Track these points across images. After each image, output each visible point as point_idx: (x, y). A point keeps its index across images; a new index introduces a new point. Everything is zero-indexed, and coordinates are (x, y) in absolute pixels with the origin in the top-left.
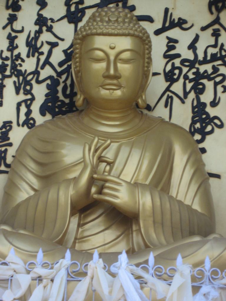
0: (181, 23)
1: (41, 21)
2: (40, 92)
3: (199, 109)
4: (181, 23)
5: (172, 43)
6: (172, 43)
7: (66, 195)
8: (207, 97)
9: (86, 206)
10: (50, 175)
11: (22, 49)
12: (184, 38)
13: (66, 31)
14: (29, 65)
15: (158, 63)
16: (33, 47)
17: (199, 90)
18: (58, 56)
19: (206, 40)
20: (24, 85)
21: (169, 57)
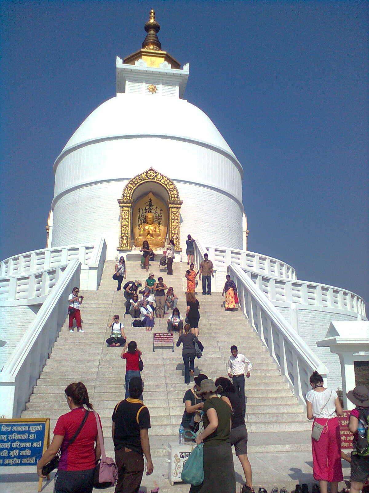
0: (157, 213)
1: (142, 213)
2: (143, 221)
3: (159, 222)
4: (157, 213)
5: (156, 215)
6: (156, 215)
7: (146, 232)
8: (160, 221)
9: (148, 234)
10: (144, 230)
11: (140, 216)
12: (157, 214)
13: (145, 214)
14: (141, 218)
15: (155, 217)
16: (142, 216)
17: (159, 220)
18: (144, 217)
19: (160, 214)
20: (141, 220)
21: (156, 216)
